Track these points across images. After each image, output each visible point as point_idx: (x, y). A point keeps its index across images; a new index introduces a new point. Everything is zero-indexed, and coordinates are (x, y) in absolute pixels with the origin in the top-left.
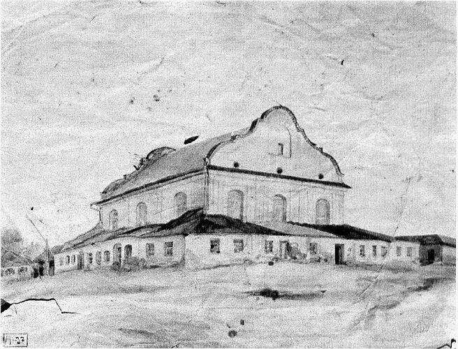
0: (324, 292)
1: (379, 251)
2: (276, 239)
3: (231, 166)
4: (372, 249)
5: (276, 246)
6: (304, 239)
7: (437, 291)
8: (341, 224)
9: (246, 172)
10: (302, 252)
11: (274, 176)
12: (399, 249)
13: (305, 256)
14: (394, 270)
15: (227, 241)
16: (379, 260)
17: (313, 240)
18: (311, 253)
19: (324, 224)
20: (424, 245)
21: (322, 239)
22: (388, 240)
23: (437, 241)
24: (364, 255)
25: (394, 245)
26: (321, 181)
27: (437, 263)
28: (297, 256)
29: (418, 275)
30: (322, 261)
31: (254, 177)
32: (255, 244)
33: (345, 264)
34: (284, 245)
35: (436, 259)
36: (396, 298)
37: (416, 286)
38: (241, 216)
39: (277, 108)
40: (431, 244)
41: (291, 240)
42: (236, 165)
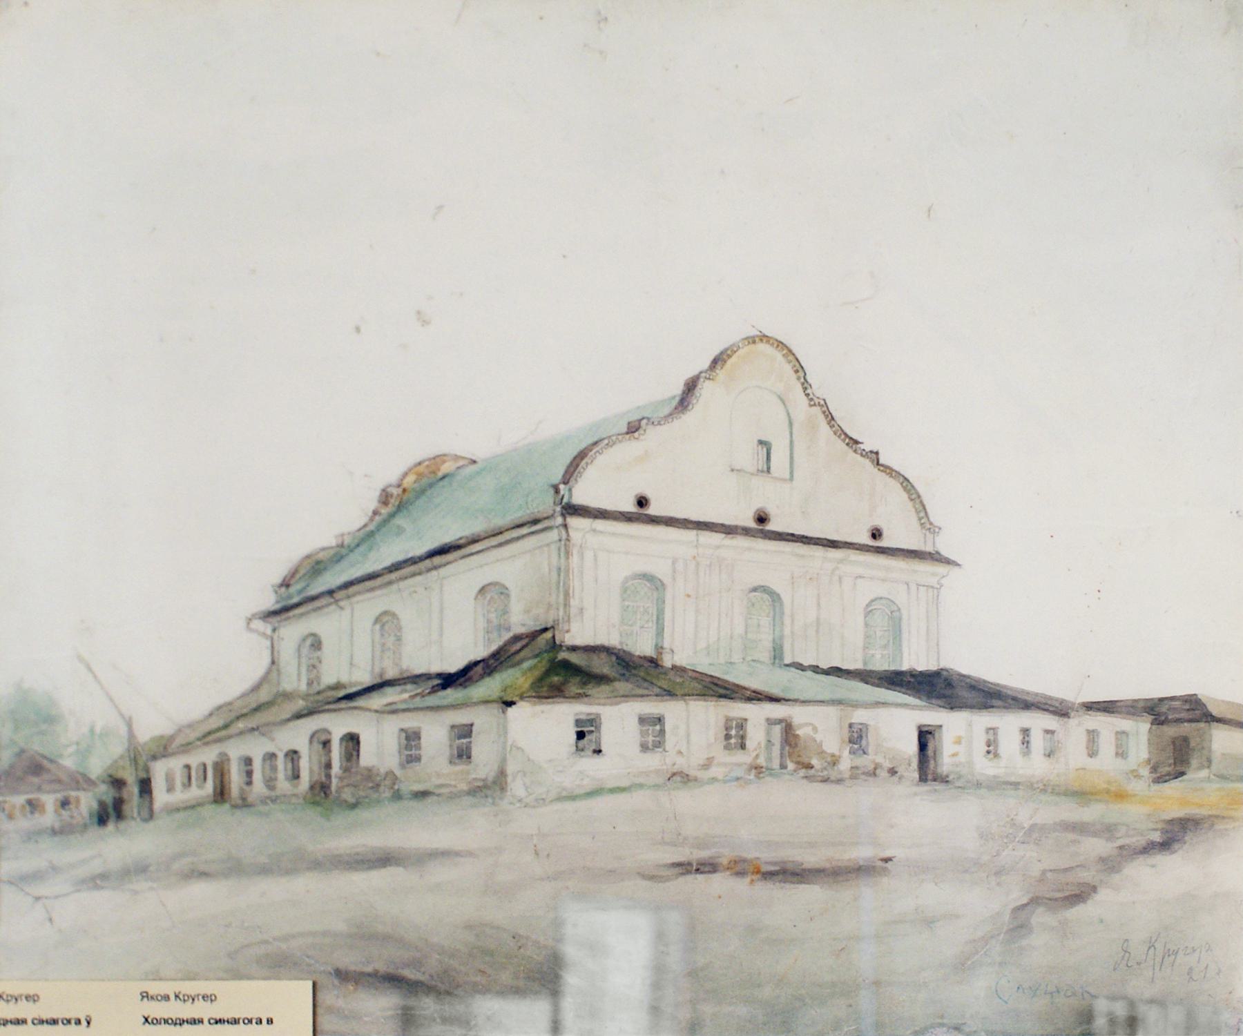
0: (887, 860)
1: (1037, 740)
2: (756, 714)
3: (630, 507)
4: (1018, 737)
5: (756, 735)
6: (832, 711)
7: (1180, 852)
8: (933, 667)
9: (670, 522)
10: (825, 748)
11: (746, 532)
12: (1092, 735)
13: (834, 761)
14: (1082, 795)
15: (619, 718)
16: (1037, 766)
17: (859, 716)
18: (852, 752)
19: (885, 667)
20: (1162, 723)
21: (882, 712)
22: (1061, 710)
23: (1196, 711)
24: (996, 755)
25: (1080, 725)
26: (874, 543)
27: (1196, 774)
28: (814, 762)
29: (1145, 809)
30: (883, 774)
31: (690, 535)
32: (694, 724)
33: (944, 780)
34: (777, 730)
35: (1194, 762)
36: (1086, 876)
37: (1140, 841)
38: (659, 649)
39: (752, 340)
40: (1179, 721)
41: (798, 715)
42: (642, 502)
